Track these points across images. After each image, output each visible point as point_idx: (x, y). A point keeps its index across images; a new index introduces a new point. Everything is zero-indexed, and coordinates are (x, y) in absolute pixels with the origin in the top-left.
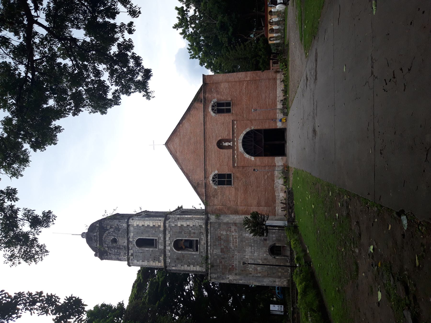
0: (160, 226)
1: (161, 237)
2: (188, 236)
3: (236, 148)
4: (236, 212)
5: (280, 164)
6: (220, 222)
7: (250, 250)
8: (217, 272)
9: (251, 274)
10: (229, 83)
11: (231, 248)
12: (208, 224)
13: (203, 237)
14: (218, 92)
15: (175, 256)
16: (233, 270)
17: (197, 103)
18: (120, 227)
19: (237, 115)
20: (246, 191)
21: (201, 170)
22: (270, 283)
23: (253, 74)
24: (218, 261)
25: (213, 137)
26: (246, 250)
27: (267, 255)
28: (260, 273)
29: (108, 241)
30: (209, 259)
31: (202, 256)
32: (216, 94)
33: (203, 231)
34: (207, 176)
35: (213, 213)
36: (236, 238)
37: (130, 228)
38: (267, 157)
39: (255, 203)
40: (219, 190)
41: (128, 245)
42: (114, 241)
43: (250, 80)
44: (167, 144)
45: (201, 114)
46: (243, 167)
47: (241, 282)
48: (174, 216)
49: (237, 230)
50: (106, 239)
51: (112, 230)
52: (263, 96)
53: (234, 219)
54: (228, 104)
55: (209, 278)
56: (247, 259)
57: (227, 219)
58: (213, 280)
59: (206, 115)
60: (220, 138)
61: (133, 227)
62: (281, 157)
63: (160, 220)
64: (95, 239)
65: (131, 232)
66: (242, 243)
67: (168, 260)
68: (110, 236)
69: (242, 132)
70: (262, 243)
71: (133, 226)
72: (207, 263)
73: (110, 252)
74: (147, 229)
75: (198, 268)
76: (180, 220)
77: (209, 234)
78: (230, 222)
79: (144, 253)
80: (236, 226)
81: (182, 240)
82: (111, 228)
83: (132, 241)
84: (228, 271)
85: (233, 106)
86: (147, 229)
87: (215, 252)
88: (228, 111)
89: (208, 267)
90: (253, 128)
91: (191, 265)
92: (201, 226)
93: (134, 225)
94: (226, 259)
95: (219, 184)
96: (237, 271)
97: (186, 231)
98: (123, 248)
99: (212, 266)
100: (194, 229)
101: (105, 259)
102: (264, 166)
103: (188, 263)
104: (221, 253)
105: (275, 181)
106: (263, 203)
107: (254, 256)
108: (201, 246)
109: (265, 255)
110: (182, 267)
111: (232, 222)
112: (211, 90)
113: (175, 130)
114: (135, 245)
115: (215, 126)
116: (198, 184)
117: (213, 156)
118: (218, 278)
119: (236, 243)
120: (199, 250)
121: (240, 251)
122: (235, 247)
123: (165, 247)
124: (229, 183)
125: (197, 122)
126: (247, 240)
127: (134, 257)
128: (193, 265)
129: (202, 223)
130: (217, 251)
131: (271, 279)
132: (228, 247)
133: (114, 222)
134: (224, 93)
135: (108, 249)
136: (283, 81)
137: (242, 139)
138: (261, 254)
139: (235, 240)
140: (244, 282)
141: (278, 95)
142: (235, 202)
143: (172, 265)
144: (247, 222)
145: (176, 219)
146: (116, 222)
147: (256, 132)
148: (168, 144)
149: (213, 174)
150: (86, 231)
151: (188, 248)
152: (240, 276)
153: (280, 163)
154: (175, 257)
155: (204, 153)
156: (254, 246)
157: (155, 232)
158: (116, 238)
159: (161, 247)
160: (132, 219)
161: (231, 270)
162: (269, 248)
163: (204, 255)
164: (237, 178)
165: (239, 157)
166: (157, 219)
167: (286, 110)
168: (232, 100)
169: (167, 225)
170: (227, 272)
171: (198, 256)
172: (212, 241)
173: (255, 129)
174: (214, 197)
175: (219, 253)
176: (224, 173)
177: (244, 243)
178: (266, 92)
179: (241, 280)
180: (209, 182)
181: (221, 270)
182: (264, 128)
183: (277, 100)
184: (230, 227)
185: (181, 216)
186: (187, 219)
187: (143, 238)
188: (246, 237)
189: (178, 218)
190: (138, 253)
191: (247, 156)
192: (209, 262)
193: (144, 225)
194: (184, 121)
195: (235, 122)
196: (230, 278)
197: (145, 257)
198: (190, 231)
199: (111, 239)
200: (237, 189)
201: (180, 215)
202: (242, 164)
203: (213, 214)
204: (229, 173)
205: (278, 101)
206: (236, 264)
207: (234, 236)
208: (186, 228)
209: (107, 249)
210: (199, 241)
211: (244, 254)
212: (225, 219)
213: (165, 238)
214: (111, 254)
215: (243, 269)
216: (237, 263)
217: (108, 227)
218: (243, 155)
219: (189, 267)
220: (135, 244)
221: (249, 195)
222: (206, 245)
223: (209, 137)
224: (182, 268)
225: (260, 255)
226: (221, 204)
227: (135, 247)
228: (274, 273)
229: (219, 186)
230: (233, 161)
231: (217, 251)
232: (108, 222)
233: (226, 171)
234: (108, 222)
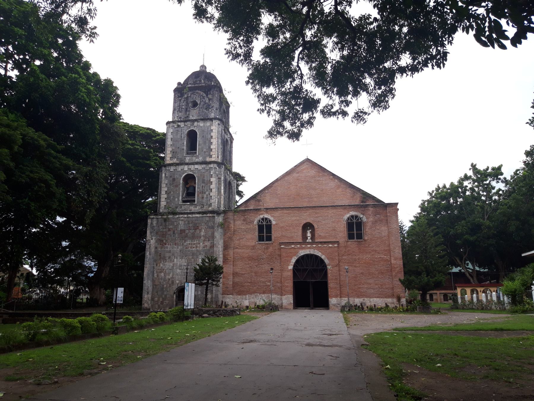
0: (211, 157)
1: (199, 158)
2: (200, 190)
3: (304, 246)
4: (226, 247)
5: (284, 301)
7: (183, 264)
9: (157, 265)
10: (387, 236)
12: (213, 213)
13: (198, 209)
14: (375, 222)
15: (176, 177)
16: (161, 244)
17: (361, 196)
18: (210, 110)
19: (346, 247)
20: (251, 258)
21: (276, 204)
23: (399, 268)
25: (316, 217)
26: (183, 260)
28: (158, 276)
29: (194, 97)
31: (177, 207)
32: (373, 221)
33: (205, 208)
34: (268, 211)
35: (225, 219)
36: (197, 247)
37: (209, 122)
38: (292, 285)
39: (237, 270)
40: (252, 226)
41: (189, 121)
42: (195, 104)
43: (391, 264)
44: (308, 161)
45: (346, 202)
46: (280, 256)
47: (147, 254)
48: (222, 173)
50: (197, 94)
51: (207, 101)
52: (371, 281)
53: (219, 244)
54: (360, 236)
55: (152, 217)
56: (173, 261)
57: (218, 237)
59: (345, 208)
60: (316, 226)
61: (210, 126)
62: (292, 302)
63: (218, 157)
64: (197, 81)
65: (204, 123)
67: (172, 169)
68: (201, 99)
69: (323, 254)
71: (211, 125)
72: (169, 213)
73: (182, 100)
74: (207, 142)
75: (163, 203)
76: (217, 180)
77: (201, 215)
79: (181, 140)
80: (211, 247)
81: (195, 183)
82: (210, 100)
83: (194, 125)
85: (356, 243)
86: (207, 142)
87: (180, 223)
88: (351, 236)
89: (164, 215)
90: (329, 267)
92: (210, 205)
93: (212, 127)
94: (173, 237)
95: (259, 226)
96: (160, 249)
98: (186, 115)
99: (165, 220)
101: (175, 95)
102: (281, 281)
105: (264, 295)
106: (237, 280)
107: (177, 269)
108: (188, 206)
109: (177, 282)
110: (165, 185)
111: (215, 242)
112: (378, 214)
113: (326, 171)
114: (190, 129)
115: (332, 220)
116: (259, 201)
117: (294, 218)
118: (152, 227)
119: (191, 248)
120: (183, 204)
121: (182, 253)
123: (187, 164)
124: (261, 239)
125: (336, 197)
126: (194, 261)
127: (176, 129)
128: (167, 197)
129: (214, 206)
131: (150, 289)
132: (186, 239)
133: (217, 102)
134: (375, 230)
135: (185, 98)
136: (387, 306)
137: (315, 254)
138: (178, 277)
140: (147, 258)
141: (372, 299)
142: (238, 246)
143: (167, 174)
144: (213, 260)
145: (219, 176)
146: (216, 105)
147: (324, 272)
148: (307, 163)
149: (272, 219)
150: (208, 71)
151: (187, 191)
153: (285, 301)
154: (176, 176)
155: (297, 207)
157: (205, 152)
158: (198, 106)
159: (187, 160)
160: (220, 123)
161: (161, 242)
163: (178, 210)
164: (267, 248)
165: (292, 251)
166: (220, 154)
167: (347, 310)
168: (365, 240)
169: (212, 166)
170: (158, 238)
171: (177, 203)
172: (194, 219)
173: (328, 270)
174: (244, 220)
175: (179, 227)
176: (273, 233)
177: (191, 257)
178: (376, 284)
179: (150, 254)
180: (262, 214)
181: (161, 230)
182: (329, 282)
183: (365, 299)
184: (209, 241)
185: (222, 182)
186: (219, 189)
187: (198, 138)
188: (197, 259)
189: (220, 178)
190: (180, 133)
191: (294, 260)
192: (170, 216)
193: (212, 138)
194: (336, 181)
195: (336, 245)
196: (152, 241)
197: (176, 141)
198: (205, 193)
199: (197, 101)
200: (253, 247)
201: (225, 180)
202: (284, 254)
203: (223, 219)
204: (273, 238)
205: (364, 300)
206: (167, 248)
207: (198, 245)
208: (208, 188)
209: (186, 96)
210: (194, 203)
211: (178, 257)
212: (218, 234)
213: (197, 163)
214: (180, 102)
215: (162, 256)
216: (168, 249)
217: (210, 96)
218: (295, 255)
219: (164, 193)
220: (191, 129)
221: (247, 263)
222: (189, 212)
223: (316, 213)
224: (163, 185)
225: (177, 276)
226: (235, 228)
227: (188, 129)
228: (157, 292)
229: (257, 227)
230: (287, 243)
231: (182, 225)
232: (216, 96)
233: (275, 234)
234: (216, 96)
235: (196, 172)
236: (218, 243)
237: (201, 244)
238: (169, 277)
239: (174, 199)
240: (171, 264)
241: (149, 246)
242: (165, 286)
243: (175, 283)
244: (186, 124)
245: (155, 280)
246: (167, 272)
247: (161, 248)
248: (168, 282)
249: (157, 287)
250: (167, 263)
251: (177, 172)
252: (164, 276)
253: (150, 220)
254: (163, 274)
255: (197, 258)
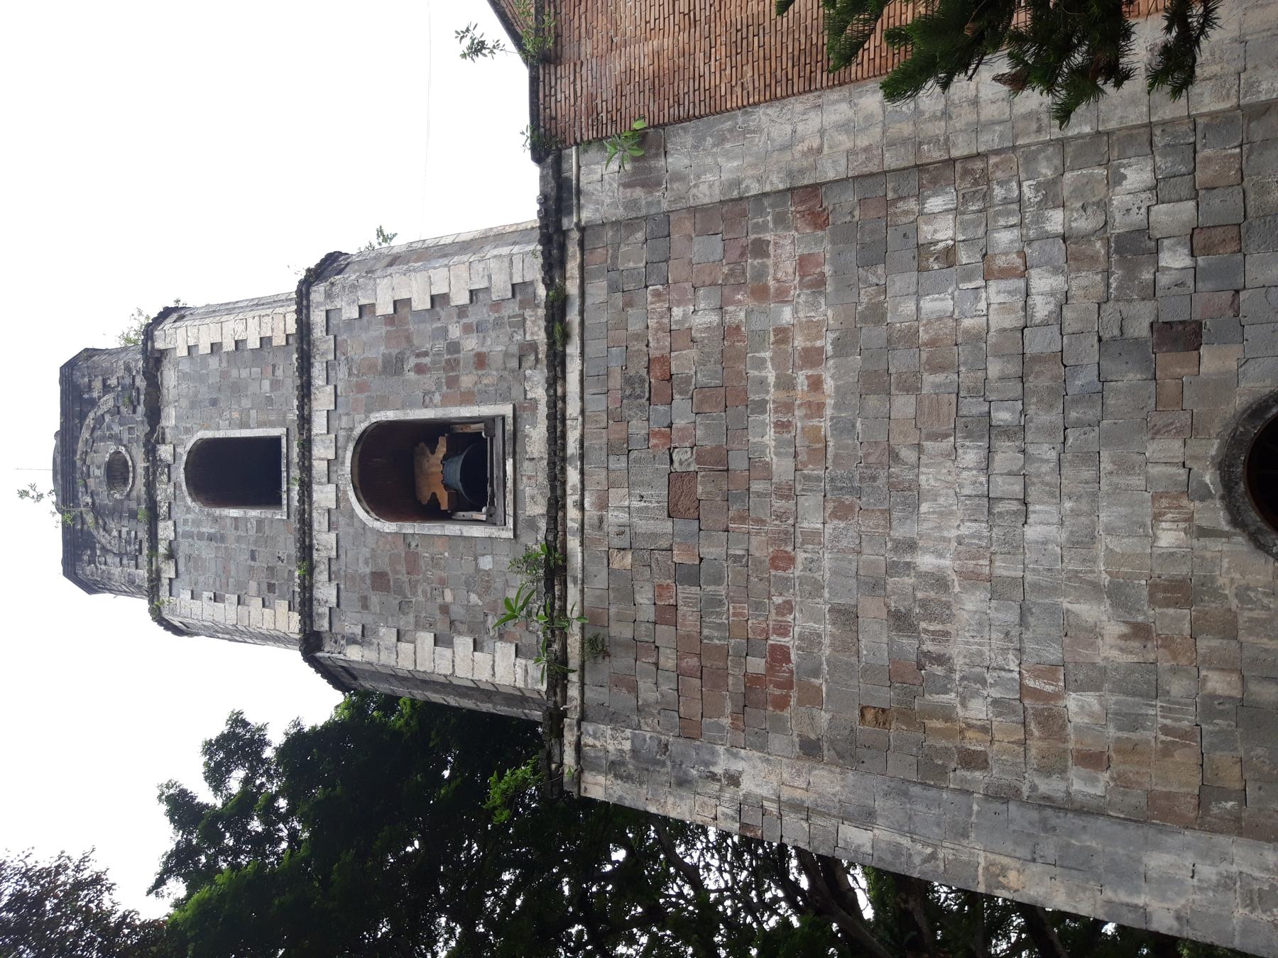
6: (665, 206)
7: (970, 481)
8: (639, 710)
9: (973, 760)
11: (767, 466)
15: (366, 563)
16: (782, 703)
22: (1240, 912)
24: (644, 597)
26: (927, 479)
27: (1203, 533)
28: (1093, 760)
30: (575, 583)
36: (812, 357)
37: (165, 372)
49: (827, 269)
53: (794, 139)
56: (940, 582)
57: (730, 166)
58: (601, 779)
66: (873, 401)
68: (103, 439)
70: (1129, 378)
77: (573, 349)
78: (755, 189)
79: (222, 538)
80: (818, 219)
83: (170, 459)
84: (728, 711)
87: (623, 517)
91: (460, 634)
94: (717, 580)
96: (824, 717)
97: (426, 354)
99: (596, 647)
100: (479, 328)
103: (438, 615)
104: (668, 526)
107: (1015, 547)
108: (527, 467)
109: (1169, 537)
110: (402, 645)
111: (777, 182)
119: (816, 409)
121: (858, 492)
122: (803, 457)
126: (941, 368)
128: (471, 631)
130: (636, 504)
132: (738, 463)
138: (1110, 531)
139: (801, 378)
140: (897, 850)
152: (850, 776)
156: (1018, 431)
162: (1234, 442)
169: (318, 317)
170: (726, 721)
172: (597, 405)
177: (903, 405)
179: (866, 818)
184: (760, 248)
188: (924, 336)
196: (747, 785)
206: (811, 641)
207: (799, 342)
208: (430, 327)
210: (509, 427)
211: (899, 532)
215: (885, 697)
216: (826, 628)
219: (447, 652)
225: (1106, 542)
235: (344, 422)
236: (784, 148)
237: (787, 315)
238: (1114, 629)
239: (481, 582)
240: (971, 603)
241: (791, 819)
242: (1218, 683)
243: (1182, 570)
244: (163, 509)
245: (1137, 798)
246: (1053, 654)
247: (812, 698)
248: (1167, 643)
249: (1231, 777)
250: (957, 651)
251: (343, 557)
252: (1092, 685)
253: (588, 777)
254: (1072, 702)
255: (909, 337)
